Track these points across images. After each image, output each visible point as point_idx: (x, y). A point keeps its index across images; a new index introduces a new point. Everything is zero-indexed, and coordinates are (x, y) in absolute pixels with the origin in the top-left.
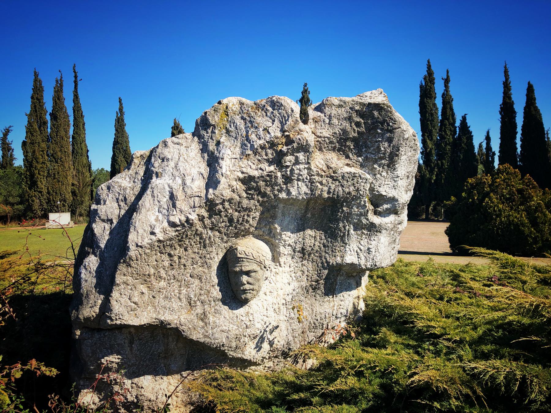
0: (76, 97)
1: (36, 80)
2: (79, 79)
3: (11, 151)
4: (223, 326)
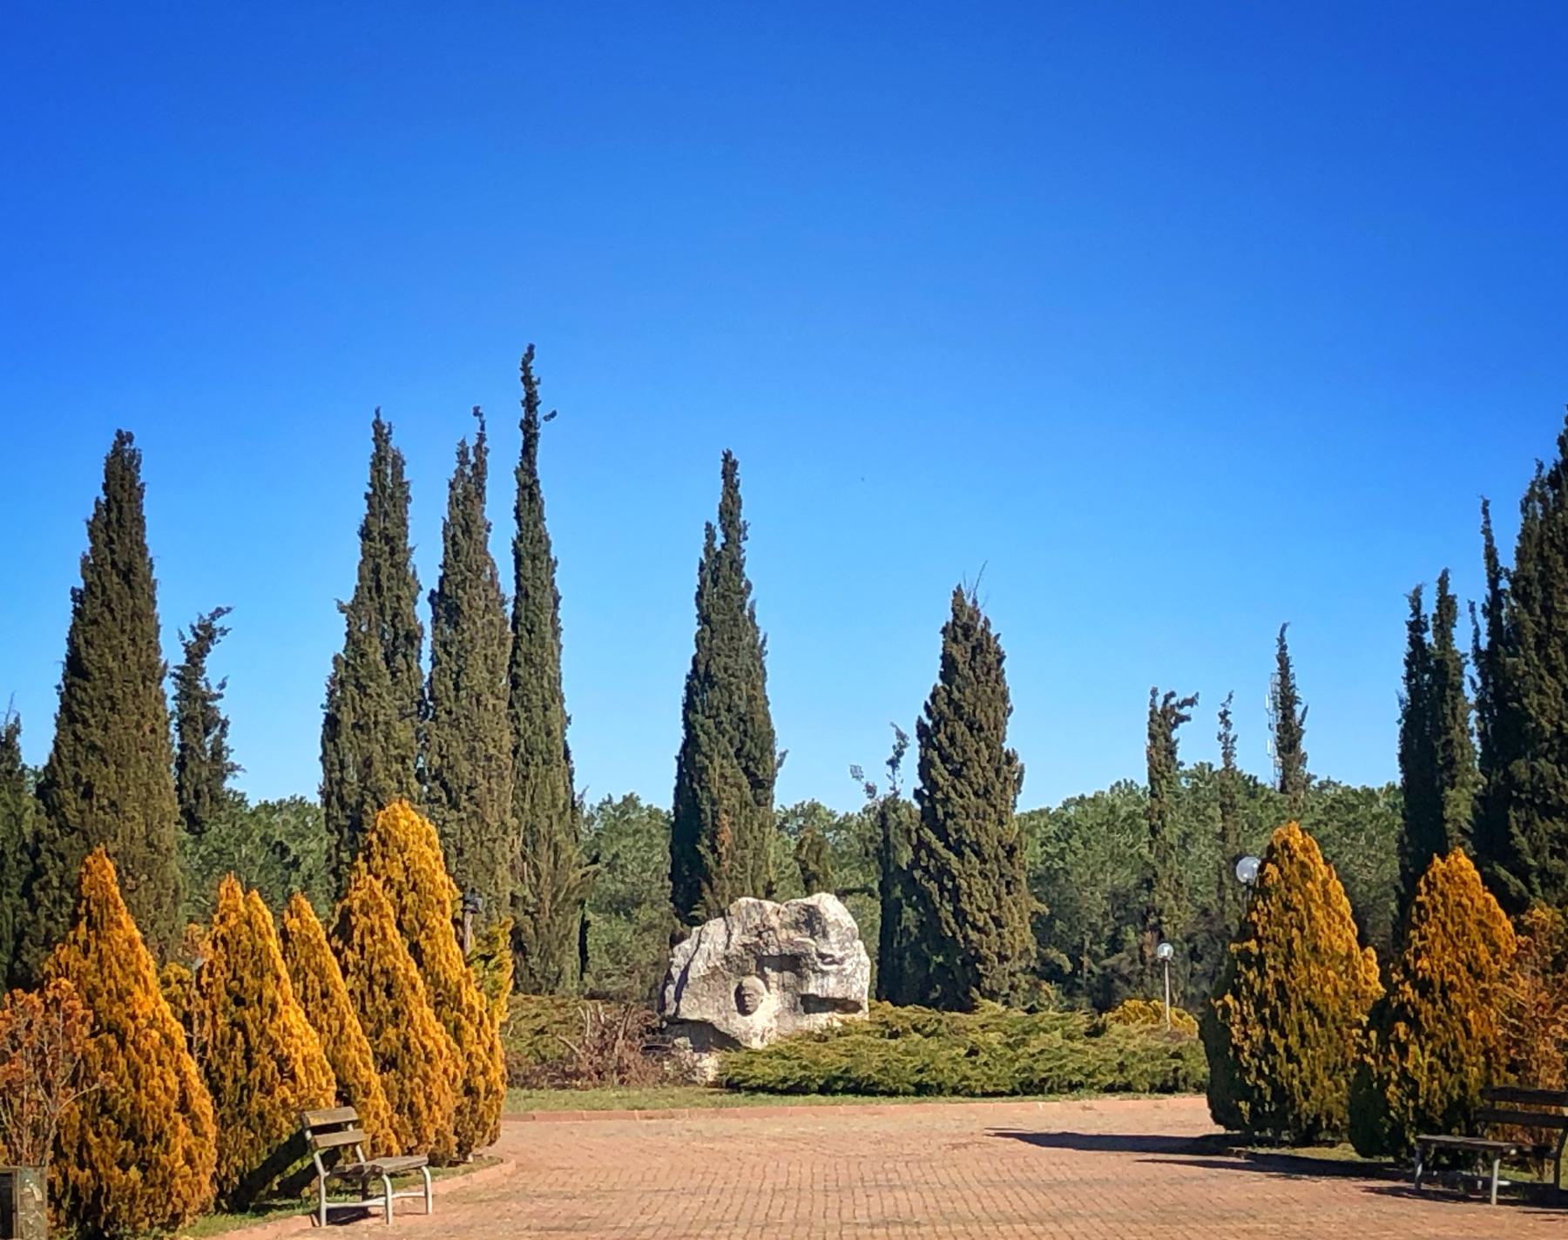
0: (529, 492)
1: (378, 461)
2: (541, 411)
3: (216, 732)
4: (737, 1024)
